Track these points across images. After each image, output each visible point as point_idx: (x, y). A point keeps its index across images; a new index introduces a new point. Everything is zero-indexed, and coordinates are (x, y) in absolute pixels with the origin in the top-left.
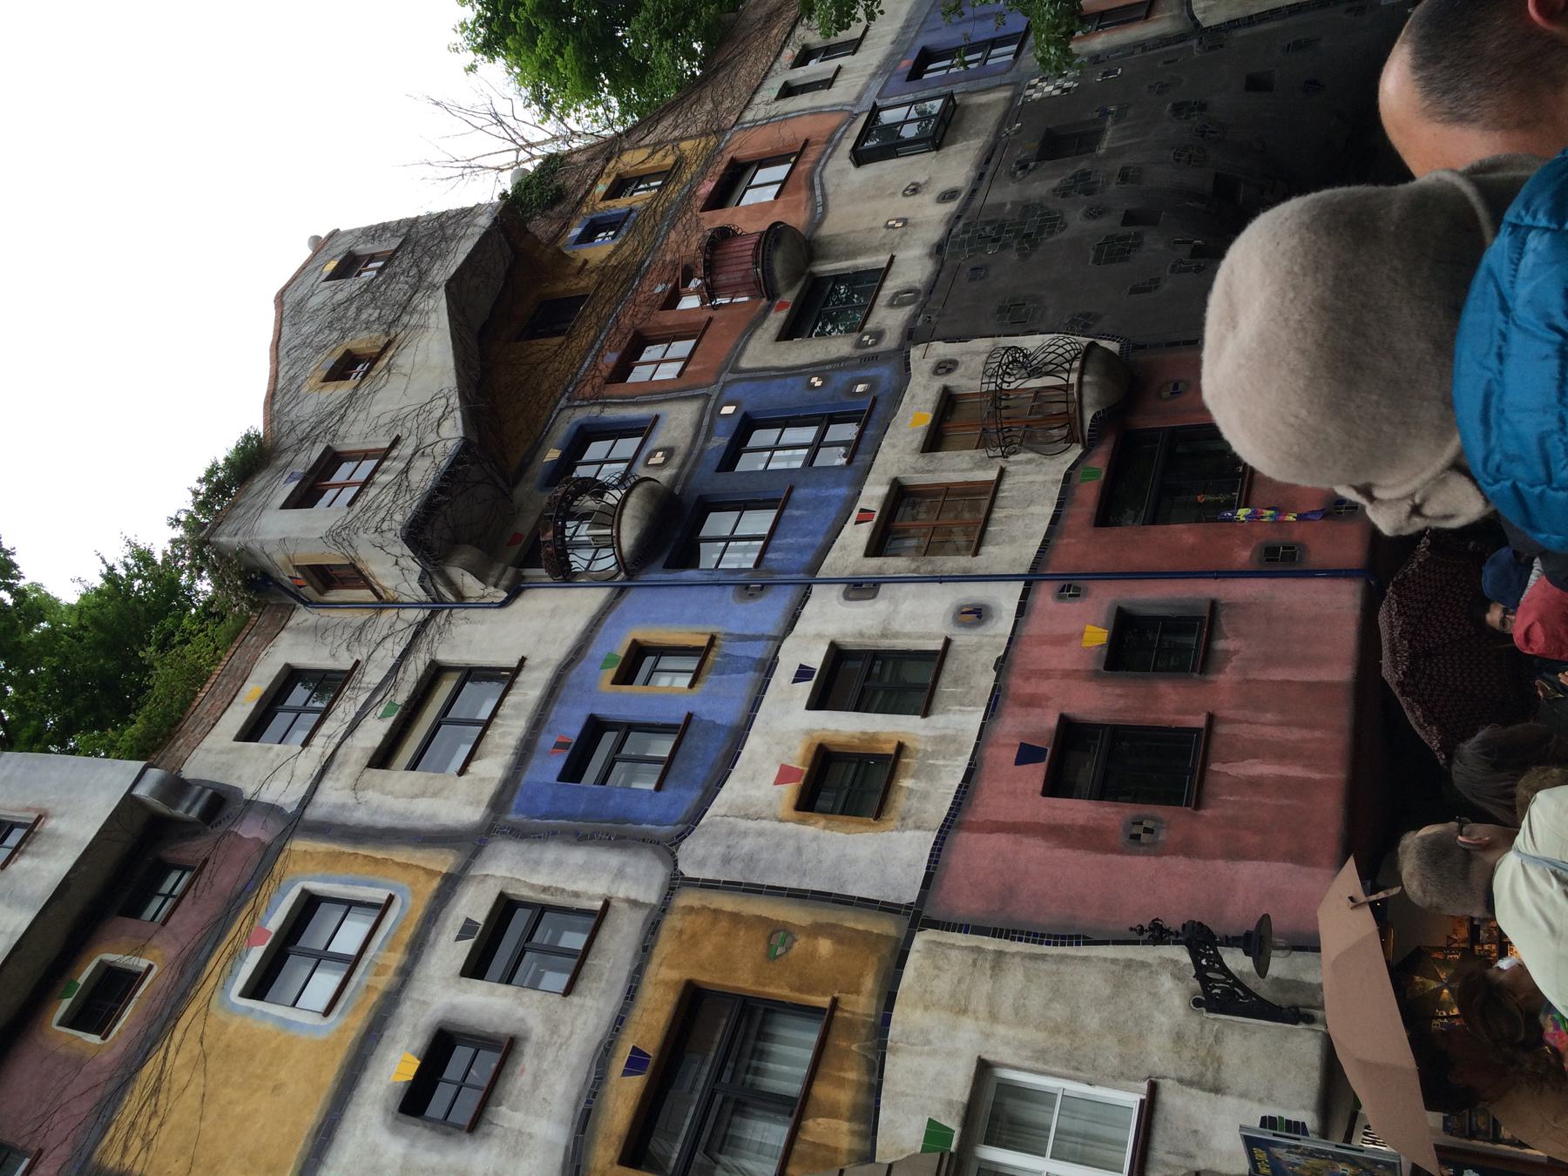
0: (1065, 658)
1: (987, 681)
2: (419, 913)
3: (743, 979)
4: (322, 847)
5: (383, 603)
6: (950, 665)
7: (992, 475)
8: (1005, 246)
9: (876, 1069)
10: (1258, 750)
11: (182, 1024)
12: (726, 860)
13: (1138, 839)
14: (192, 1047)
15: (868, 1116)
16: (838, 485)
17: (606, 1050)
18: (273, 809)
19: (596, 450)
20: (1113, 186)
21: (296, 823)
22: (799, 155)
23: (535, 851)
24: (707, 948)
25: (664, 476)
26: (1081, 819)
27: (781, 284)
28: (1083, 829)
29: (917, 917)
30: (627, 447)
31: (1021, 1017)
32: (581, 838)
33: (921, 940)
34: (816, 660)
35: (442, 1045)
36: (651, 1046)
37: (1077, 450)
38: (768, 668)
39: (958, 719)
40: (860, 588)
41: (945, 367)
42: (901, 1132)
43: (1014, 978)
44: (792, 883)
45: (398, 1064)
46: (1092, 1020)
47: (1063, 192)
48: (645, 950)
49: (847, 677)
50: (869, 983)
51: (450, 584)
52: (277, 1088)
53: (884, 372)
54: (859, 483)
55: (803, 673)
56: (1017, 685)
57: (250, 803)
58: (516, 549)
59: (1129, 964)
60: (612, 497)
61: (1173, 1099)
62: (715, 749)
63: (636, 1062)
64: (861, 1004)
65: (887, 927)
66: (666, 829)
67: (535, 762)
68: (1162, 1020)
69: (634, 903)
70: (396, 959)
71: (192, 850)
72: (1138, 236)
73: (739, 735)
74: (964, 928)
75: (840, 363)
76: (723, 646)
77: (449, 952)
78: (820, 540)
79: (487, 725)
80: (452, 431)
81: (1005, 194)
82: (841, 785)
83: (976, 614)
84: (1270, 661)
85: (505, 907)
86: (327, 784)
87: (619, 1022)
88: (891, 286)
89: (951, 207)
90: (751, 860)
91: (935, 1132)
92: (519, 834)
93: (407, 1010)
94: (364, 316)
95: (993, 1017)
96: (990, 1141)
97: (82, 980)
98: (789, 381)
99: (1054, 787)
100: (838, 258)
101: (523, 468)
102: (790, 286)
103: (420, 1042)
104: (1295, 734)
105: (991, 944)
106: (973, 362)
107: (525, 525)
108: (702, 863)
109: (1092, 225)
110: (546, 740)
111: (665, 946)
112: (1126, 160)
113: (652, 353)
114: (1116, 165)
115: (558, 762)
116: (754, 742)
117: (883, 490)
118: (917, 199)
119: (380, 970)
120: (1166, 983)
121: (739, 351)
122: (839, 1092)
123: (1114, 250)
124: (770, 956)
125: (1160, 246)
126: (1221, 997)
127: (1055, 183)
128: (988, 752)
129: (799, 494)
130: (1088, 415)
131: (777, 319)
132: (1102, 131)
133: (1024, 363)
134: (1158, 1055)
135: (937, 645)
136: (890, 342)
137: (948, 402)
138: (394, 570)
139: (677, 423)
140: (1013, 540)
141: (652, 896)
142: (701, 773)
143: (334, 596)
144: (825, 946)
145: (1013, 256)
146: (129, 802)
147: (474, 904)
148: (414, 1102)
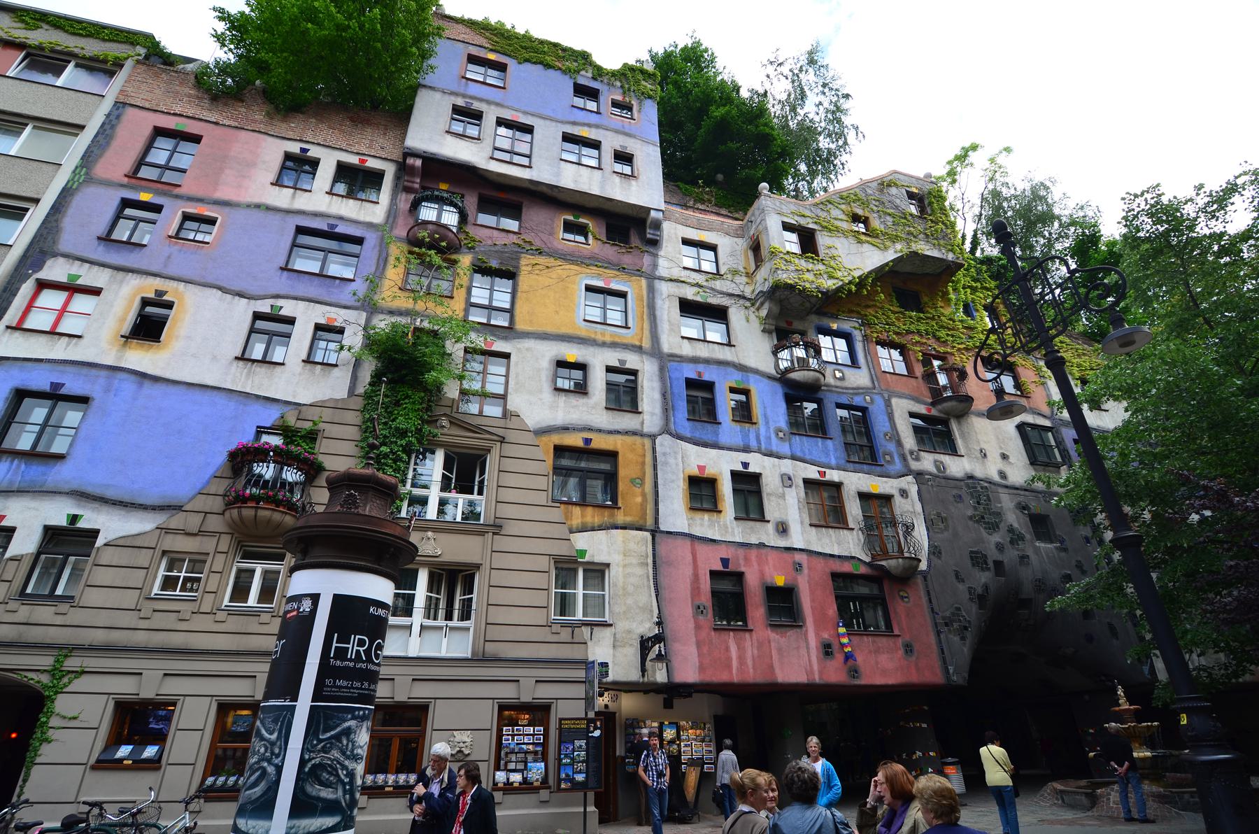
0: (769, 570)
1: (754, 540)
2: (625, 341)
3: (623, 472)
4: (645, 293)
5: (750, 275)
6: (758, 524)
7: (851, 526)
8: (975, 509)
9: (600, 528)
10: (741, 648)
11: (572, 267)
12: (664, 454)
13: (699, 609)
14: (565, 273)
15: (583, 529)
16: (836, 458)
17: (590, 429)
18: (655, 266)
19: (841, 344)
20: (1016, 553)
21: (652, 278)
22: (1022, 396)
23: (656, 378)
24: (630, 456)
25: (830, 380)
26: (702, 586)
27: (940, 407)
28: (698, 588)
29: (655, 532)
30: (843, 357)
31: (627, 576)
32: (664, 395)
33: (648, 535)
34: (751, 469)
35: (582, 367)
36: (594, 445)
37: (868, 559)
38: (746, 449)
39: (738, 532)
40: (787, 480)
41: (904, 493)
42: (581, 541)
43: (639, 571)
44: (660, 482)
45: (572, 353)
46: (630, 601)
47: (1011, 530)
48: (626, 433)
49: (747, 483)
50: (629, 519)
51: (762, 304)
52: (557, 312)
53: (898, 466)
54: (838, 468)
55: (746, 465)
56: (753, 553)
57: (656, 256)
58: (783, 325)
59: (651, 611)
60: (813, 363)
61: (608, 632)
62: (709, 438)
63: (588, 441)
64: (620, 518)
65: (650, 522)
66: (672, 427)
67: (691, 366)
68: (634, 626)
69: (642, 423)
70: (608, 339)
71: (635, 241)
72: (988, 569)
73: (715, 446)
74: (654, 549)
75: (899, 444)
76: (752, 428)
77: (613, 358)
78: (808, 457)
79: (705, 341)
80: (830, 284)
81: (1007, 502)
82: (702, 490)
83: (783, 529)
84: (780, 650)
85: (634, 373)
86: (670, 284)
87: (600, 431)
88: (947, 459)
89: (997, 478)
90: (666, 463)
91: (583, 553)
92: (662, 369)
93: (591, 349)
94: (888, 218)
95: (625, 566)
96: (584, 571)
97: (581, 220)
98: (887, 424)
99: (714, 574)
100: (959, 429)
101: (825, 314)
102: (940, 411)
103: (581, 360)
104: (750, 662)
105: (650, 560)
106: (909, 508)
107: (797, 325)
108: (662, 445)
109: (993, 547)
110: (701, 367)
111: (629, 439)
112: (1033, 557)
113: (895, 354)
114: (1030, 552)
115: (693, 376)
116: (714, 452)
117: (836, 479)
118: (999, 459)
119: (603, 335)
120: (648, 625)
121: (900, 396)
122: (592, 516)
123: (978, 559)
124: (632, 481)
125: (983, 580)
126: (645, 645)
127: (1016, 525)
128: (723, 546)
129: (829, 443)
130: (883, 563)
131: (922, 409)
132: (1052, 542)
133: (909, 528)
134: (621, 626)
135: (767, 518)
136: (915, 465)
137: (887, 499)
138: (764, 279)
139: (859, 378)
140: (820, 540)
141: (646, 430)
142: (697, 435)
143: (750, 254)
144: (639, 499)
145: (970, 512)
146: (648, 210)
147: (632, 361)
148: (561, 364)
